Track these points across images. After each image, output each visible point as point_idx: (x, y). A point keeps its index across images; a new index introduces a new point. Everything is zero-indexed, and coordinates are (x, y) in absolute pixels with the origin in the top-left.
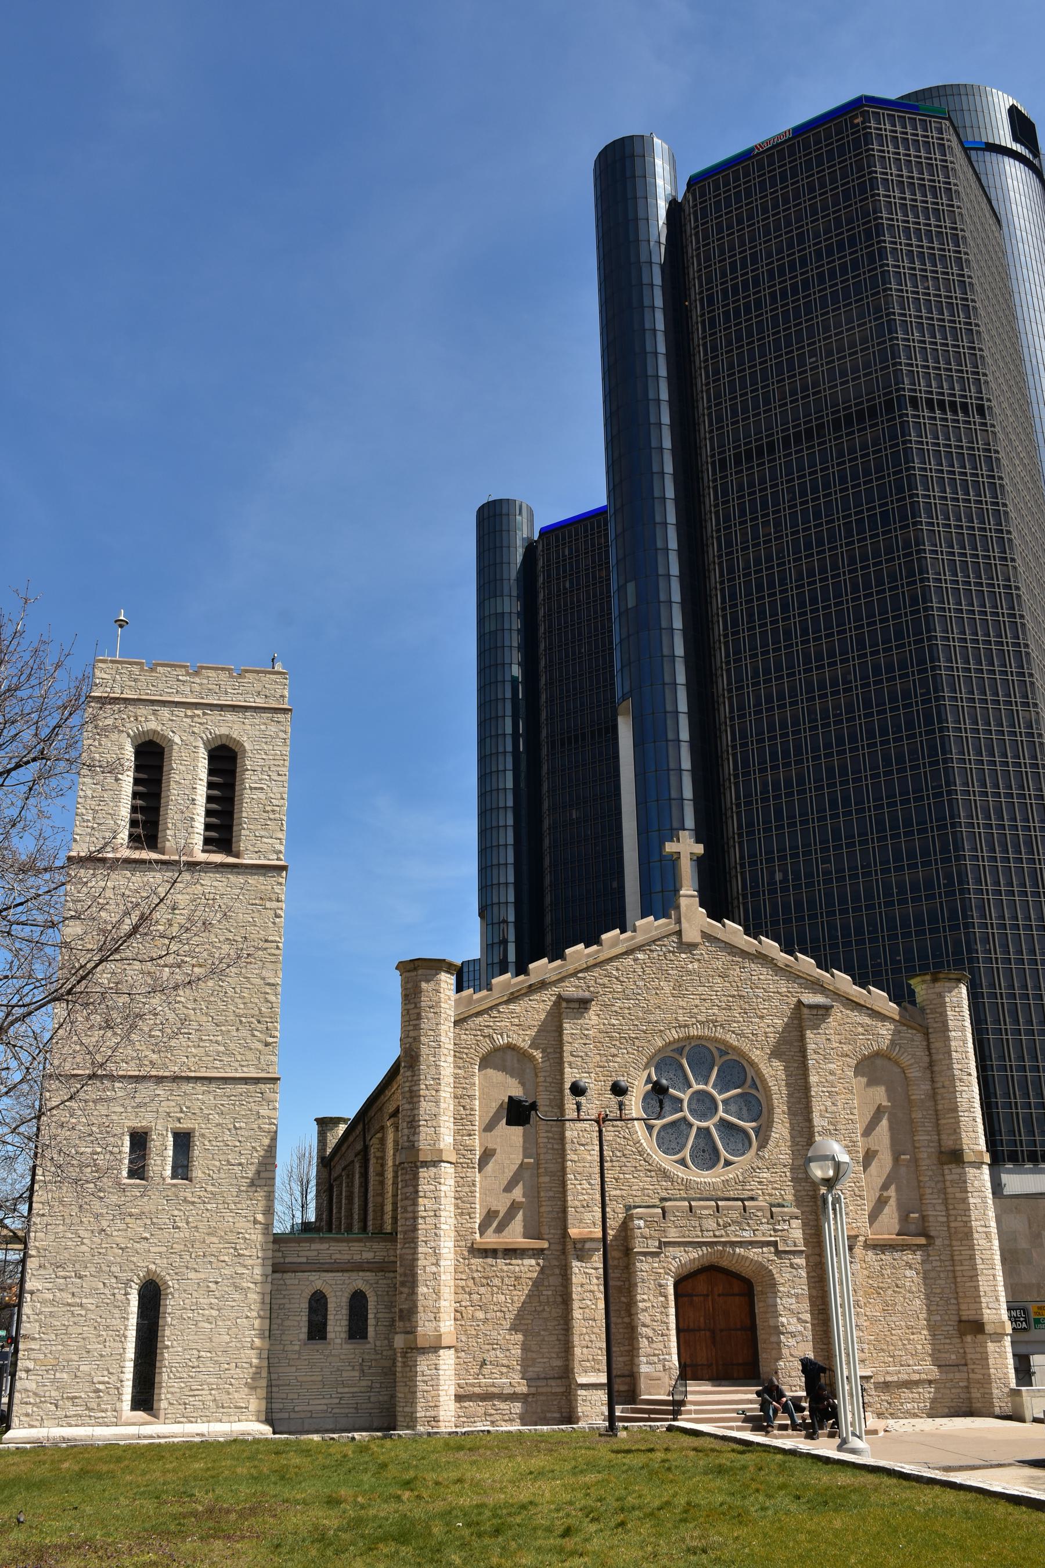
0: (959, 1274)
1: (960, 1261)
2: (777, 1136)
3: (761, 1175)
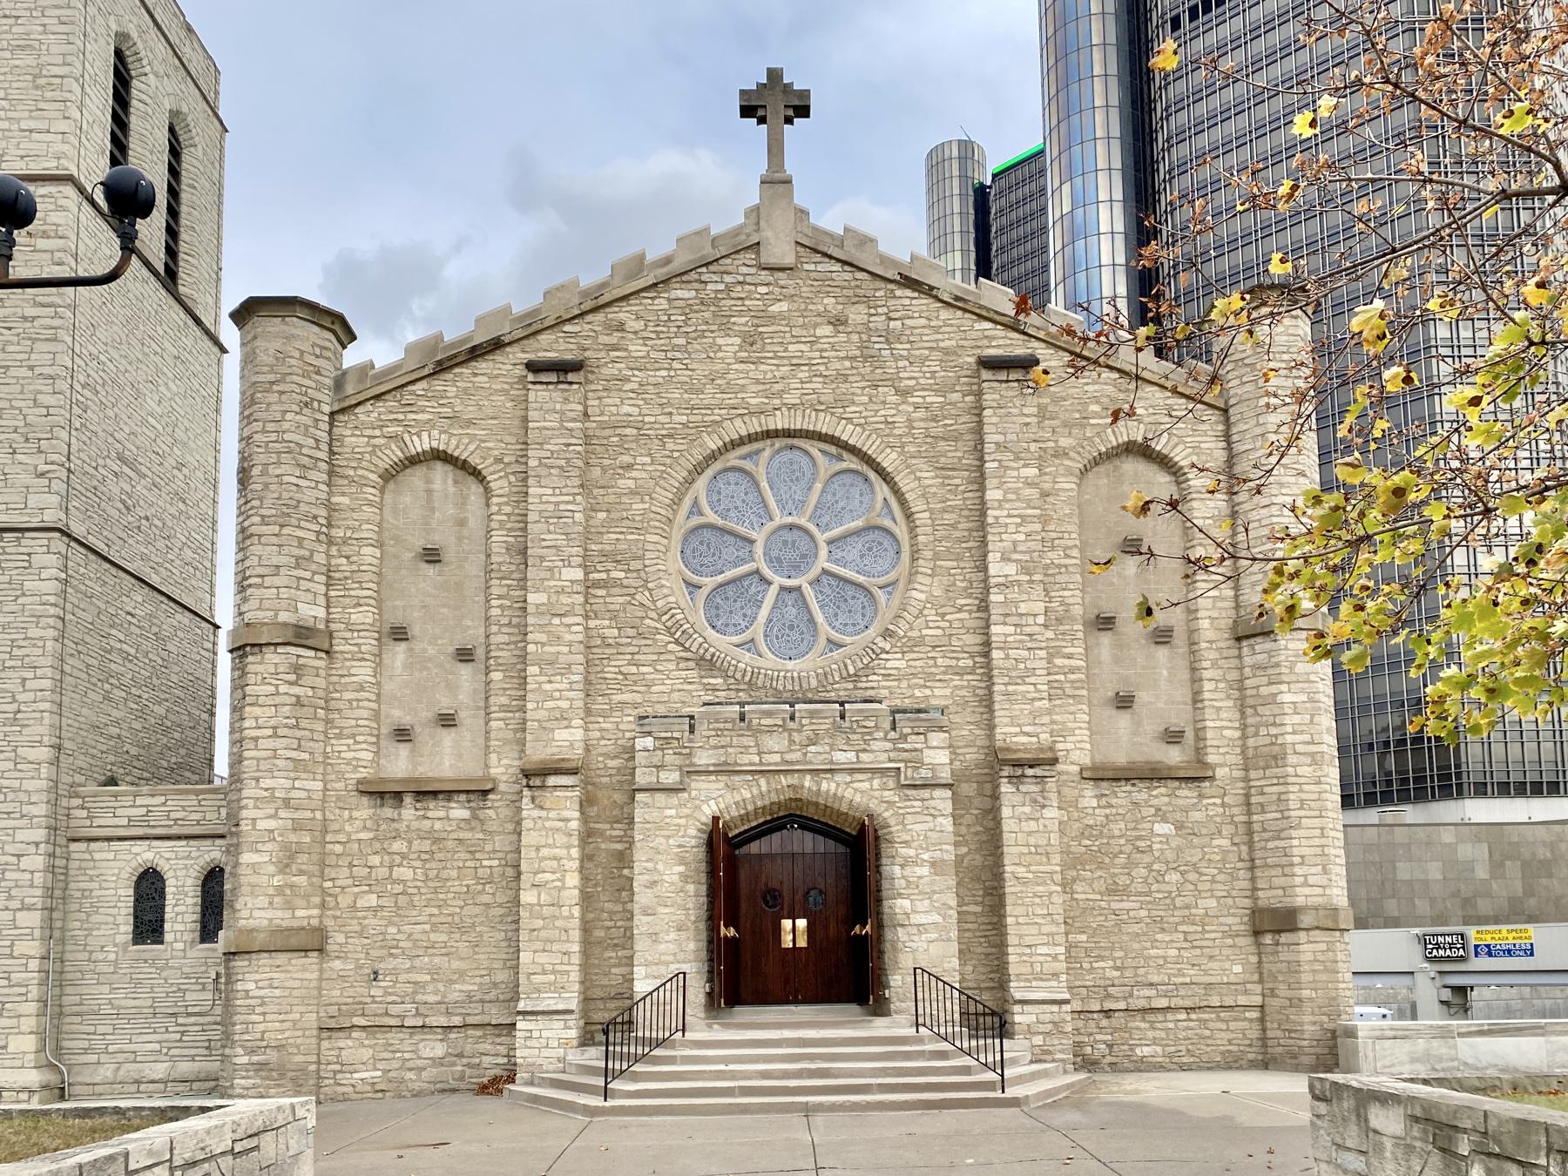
0: (1256, 827)
1: (1262, 805)
2: (923, 597)
3: (889, 665)
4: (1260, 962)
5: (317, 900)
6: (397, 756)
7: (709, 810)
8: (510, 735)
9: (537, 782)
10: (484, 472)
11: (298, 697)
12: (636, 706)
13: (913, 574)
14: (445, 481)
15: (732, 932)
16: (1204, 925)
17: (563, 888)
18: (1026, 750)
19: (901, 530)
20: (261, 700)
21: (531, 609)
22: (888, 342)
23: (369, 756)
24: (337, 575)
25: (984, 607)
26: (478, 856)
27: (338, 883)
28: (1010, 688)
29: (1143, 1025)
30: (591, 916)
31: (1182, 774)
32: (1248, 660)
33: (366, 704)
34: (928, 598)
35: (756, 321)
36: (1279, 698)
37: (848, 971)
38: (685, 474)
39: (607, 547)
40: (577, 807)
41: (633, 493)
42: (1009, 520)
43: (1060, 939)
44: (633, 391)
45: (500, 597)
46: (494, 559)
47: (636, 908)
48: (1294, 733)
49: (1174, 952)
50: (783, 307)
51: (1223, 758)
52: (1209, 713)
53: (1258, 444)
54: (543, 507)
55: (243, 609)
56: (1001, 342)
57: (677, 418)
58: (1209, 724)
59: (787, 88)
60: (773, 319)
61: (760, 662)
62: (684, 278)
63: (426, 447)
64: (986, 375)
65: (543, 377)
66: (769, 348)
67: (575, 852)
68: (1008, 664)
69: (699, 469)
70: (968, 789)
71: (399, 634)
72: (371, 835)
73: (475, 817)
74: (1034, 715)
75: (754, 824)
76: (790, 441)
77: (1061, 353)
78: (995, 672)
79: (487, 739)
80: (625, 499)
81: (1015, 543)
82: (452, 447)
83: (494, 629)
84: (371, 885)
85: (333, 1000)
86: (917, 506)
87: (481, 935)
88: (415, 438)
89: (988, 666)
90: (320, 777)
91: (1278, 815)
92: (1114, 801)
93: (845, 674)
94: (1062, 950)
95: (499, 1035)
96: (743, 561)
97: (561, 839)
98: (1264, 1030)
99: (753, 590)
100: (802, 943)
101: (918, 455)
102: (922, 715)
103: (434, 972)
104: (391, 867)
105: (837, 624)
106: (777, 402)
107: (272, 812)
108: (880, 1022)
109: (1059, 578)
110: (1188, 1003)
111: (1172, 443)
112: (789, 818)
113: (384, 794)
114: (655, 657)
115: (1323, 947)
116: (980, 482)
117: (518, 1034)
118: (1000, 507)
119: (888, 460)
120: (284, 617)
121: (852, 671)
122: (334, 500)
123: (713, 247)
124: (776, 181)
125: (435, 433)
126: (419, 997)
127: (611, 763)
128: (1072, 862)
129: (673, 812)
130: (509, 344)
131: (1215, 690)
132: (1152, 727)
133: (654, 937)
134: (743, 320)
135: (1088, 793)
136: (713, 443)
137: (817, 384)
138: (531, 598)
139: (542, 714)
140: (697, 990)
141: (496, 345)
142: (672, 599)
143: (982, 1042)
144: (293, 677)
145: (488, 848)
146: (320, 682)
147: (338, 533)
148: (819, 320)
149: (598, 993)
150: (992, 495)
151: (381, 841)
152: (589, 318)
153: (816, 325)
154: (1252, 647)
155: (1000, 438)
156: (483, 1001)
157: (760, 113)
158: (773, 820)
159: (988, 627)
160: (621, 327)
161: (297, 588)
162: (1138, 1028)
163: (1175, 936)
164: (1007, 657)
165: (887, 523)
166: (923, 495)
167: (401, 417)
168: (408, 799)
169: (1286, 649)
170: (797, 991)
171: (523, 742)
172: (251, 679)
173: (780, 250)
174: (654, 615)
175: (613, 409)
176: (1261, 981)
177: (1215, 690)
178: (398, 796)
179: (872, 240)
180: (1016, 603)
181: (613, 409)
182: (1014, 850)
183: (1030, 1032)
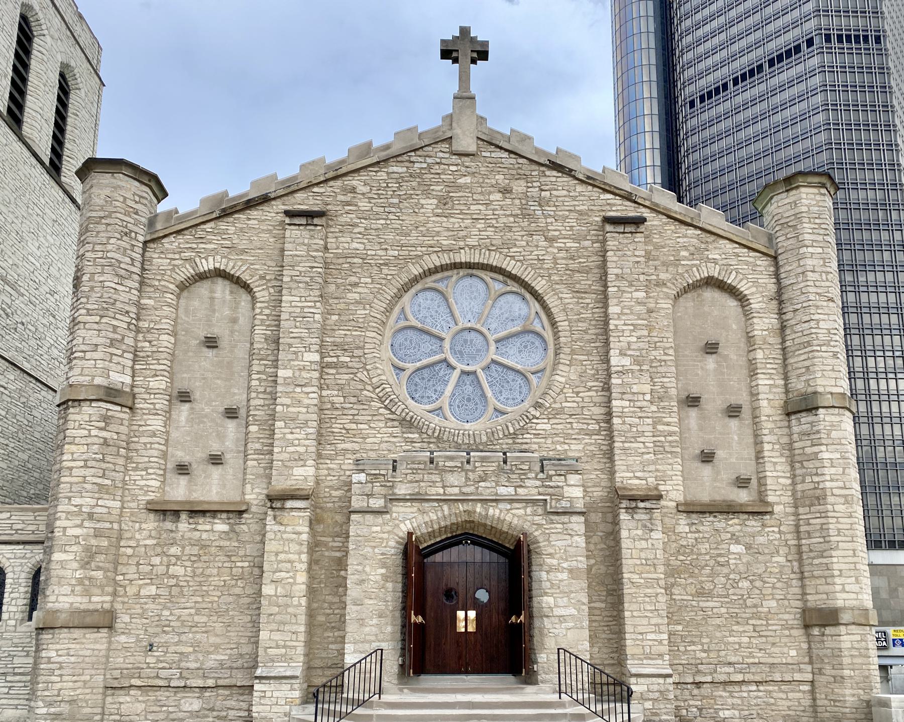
0: (804, 548)
1: (808, 532)
2: (563, 380)
3: (538, 427)
4: (810, 648)
5: (110, 589)
6: (179, 484)
7: (405, 528)
8: (261, 471)
10: (251, 286)
11: (105, 439)
12: (354, 452)
13: (556, 364)
14: (223, 291)
15: (420, 619)
16: (767, 620)
17: (295, 583)
18: (638, 490)
19: (548, 335)
20: (77, 440)
21: (280, 381)
22: (540, 205)
23: (158, 484)
24: (141, 354)
25: (607, 388)
26: (233, 559)
27: (127, 577)
28: (626, 445)
29: (724, 694)
30: (315, 605)
31: (750, 509)
32: (796, 429)
33: (156, 446)
35: (448, 189)
36: (820, 456)
37: (507, 650)
38: (395, 291)
39: (338, 340)
40: (307, 524)
41: (358, 302)
42: (625, 328)
43: (664, 628)
44: (360, 233)
45: (258, 373)
46: (256, 346)
47: (348, 600)
48: (832, 480)
49: (746, 640)
50: (468, 180)
51: (779, 497)
52: (768, 467)
53: (800, 279)
55: (70, 375)
56: (619, 208)
57: (391, 253)
58: (768, 474)
59: (473, 40)
61: (446, 424)
62: (399, 159)
63: (211, 267)
64: (609, 228)
65: (297, 221)
67: (304, 557)
69: (405, 288)
70: (596, 517)
71: (185, 397)
72: (154, 542)
73: (233, 530)
75: (438, 539)
76: (470, 271)
77: (660, 216)
78: (616, 433)
79: (245, 474)
80: (352, 307)
81: (629, 343)
83: (253, 395)
84: (152, 578)
85: (117, 666)
86: (559, 317)
87: (233, 617)
88: (203, 261)
89: (610, 429)
90: (119, 498)
91: (822, 540)
92: (701, 528)
93: (507, 433)
94: (665, 636)
95: (242, 694)
96: (436, 353)
97: (294, 547)
98: (814, 699)
99: (442, 373)
100: (471, 628)
101: (560, 282)
102: (563, 462)
103: (196, 645)
104: (168, 566)
105: (502, 398)
106: (462, 244)
107: (79, 522)
108: (530, 689)
110: (758, 678)
111: (738, 279)
112: (464, 535)
113: (166, 512)
114: (370, 418)
115: (858, 638)
117: (255, 694)
118: (619, 318)
119: (540, 285)
120: (98, 381)
121: (512, 431)
122: (142, 301)
123: (419, 139)
124: (464, 98)
125: (218, 258)
126: (183, 664)
127: (334, 493)
128: (672, 572)
129: (378, 529)
130: (274, 199)
131: (772, 450)
132: (727, 476)
133: (361, 622)
134: (439, 188)
135: (682, 522)
136: (416, 270)
137: (490, 232)
138: (281, 373)
139: (285, 456)
140: (392, 663)
141: (265, 199)
142: (383, 377)
143: (606, 706)
144: (102, 424)
145: (241, 553)
146: (124, 429)
147: (144, 325)
148: (492, 189)
149: (317, 663)
150: (613, 310)
151: (162, 544)
152: (331, 183)
153: (490, 193)
154: (799, 419)
155: (619, 271)
156: (231, 668)
157: (454, 55)
158: (452, 537)
159: (610, 401)
160: (353, 190)
161: (110, 361)
162: (721, 697)
163: (747, 628)
164: (624, 423)
165: (538, 327)
166: (564, 310)
167: (194, 246)
168: (184, 516)
169: (824, 420)
170: (467, 665)
171: (269, 477)
172: (71, 425)
173: (467, 143)
175: (346, 245)
176: (811, 663)
177: (772, 450)
178: (176, 513)
179: (530, 138)
180: (630, 385)
181: (346, 245)
182: (630, 562)
183: (643, 698)
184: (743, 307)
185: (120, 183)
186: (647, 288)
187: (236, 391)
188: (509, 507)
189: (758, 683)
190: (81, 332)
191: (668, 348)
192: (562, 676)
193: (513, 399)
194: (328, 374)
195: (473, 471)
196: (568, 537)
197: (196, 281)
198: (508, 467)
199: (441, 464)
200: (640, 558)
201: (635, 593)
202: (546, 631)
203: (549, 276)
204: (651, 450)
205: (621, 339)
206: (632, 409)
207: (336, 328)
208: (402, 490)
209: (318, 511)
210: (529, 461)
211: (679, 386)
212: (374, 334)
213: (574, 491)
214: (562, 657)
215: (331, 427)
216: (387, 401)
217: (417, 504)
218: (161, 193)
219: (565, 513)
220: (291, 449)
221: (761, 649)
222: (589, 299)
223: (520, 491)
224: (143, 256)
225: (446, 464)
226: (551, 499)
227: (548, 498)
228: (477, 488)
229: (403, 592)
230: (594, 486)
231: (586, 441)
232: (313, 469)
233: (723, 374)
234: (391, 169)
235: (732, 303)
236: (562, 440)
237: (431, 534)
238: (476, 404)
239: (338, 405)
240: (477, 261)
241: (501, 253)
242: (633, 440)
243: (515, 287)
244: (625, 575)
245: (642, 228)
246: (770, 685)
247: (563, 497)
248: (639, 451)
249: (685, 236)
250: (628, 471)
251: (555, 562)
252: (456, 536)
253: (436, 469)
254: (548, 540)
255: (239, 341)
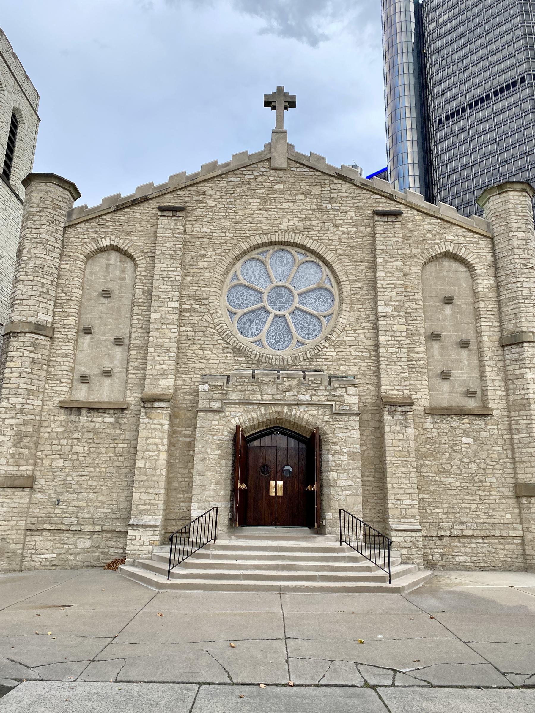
0: (515, 441)
1: (518, 429)
2: (345, 321)
3: (328, 354)
4: (520, 513)
5: (32, 461)
7: (235, 422)
8: (137, 381)
9: (149, 405)
10: (134, 256)
11: (33, 358)
13: (340, 310)
14: (116, 260)
15: (244, 486)
16: (490, 492)
17: (158, 460)
18: (397, 398)
19: (335, 290)
20: (15, 359)
21: (152, 321)
22: (330, 203)
23: (66, 389)
24: (60, 301)
25: (375, 327)
26: (116, 442)
27: (44, 453)
28: (389, 367)
29: (459, 545)
30: (172, 475)
31: (476, 413)
32: (508, 357)
33: (67, 363)
34: (349, 322)
35: (267, 192)
36: (525, 376)
37: (304, 510)
38: (231, 260)
39: (192, 293)
40: (168, 418)
41: (205, 268)
42: (388, 286)
43: (415, 496)
44: (208, 222)
45: (138, 315)
46: (136, 297)
47: (195, 472)
49: (474, 506)
50: (281, 186)
51: (496, 403)
52: (489, 383)
53: (509, 253)
54: (161, 273)
55: (12, 315)
56: (384, 205)
57: (228, 235)
58: (489, 388)
59: (286, 95)
60: (276, 191)
62: (235, 172)
63: (108, 244)
64: (377, 218)
65: (166, 214)
66: (273, 204)
67: (165, 441)
68: (389, 355)
69: (238, 258)
70: (367, 417)
71: (87, 331)
72: (63, 429)
73: (117, 422)
74: (401, 380)
75: (258, 430)
76: (282, 247)
77: (412, 210)
78: (381, 359)
79: (126, 383)
80: (201, 271)
81: (391, 296)
82: (120, 244)
83: (134, 330)
84: (61, 454)
85: (35, 515)
86: (343, 278)
87: (115, 483)
88: (103, 240)
89: (378, 356)
90: (41, 399)
91: (527, 435)
92: (442, 426)
93: (305, 358)
94: (416, 502)
95: (119, 537)
96: (257, 302)
97: (159, 434)
98: (524, 550)
102: (344, 379)
103: (89, 501)
104: (72, 446)
105: (302, 334)
106: (276, 228)
107: (14, 415)
108: (320, 538)
109: (412, 314)
110: (483, 533)
111: (467, 253)
112: (275, 428)
113: (71, 408)
114: (212, 346)
116: (374, 267)
117: (129, 537)
118: (384, 280)
119: (329, 257)
120: (30, 319)
121: (309, 356)
122: (62, 266)
123: (249, 159)
124: (280, 132)
125: (113, 238)
126: (80, 515)
127: (187, 397)
128: (421, 456)
129: (216, 423)
130: (151, 199)
131: (492, 371)
132: (460, 389)
133: (203, 487)
134: (262, 191)
135: (428, 421)
136: (245, 246)
137: (296, 220)
138: (153, 315)
139: (154, 372)
140: (224, 517)
142: (222, 319)
144: (32, 349)
145: (122, 438)
146: (46, 352)
148: (297, 192)
149: (173, 516)
151: (68, 432)
152: (189, 189)
153: (296, 195)
154: (510, 350)
155: (384, 247)
156: (112, 518)
157: (273, 104)
158: (267, 429)
159: (377, 337)
160: (204, 193)
161: (39, 306)
162: (457, 546)
163: (475, 497)
165: (328, 286)
166: (346, 274)
167: (97, 230)
168: (84, 412)
169: (528, 351)
170: (277, 519)
171: (143, 385)
172: (11, 349)
173: (281, 161)
174: (212, 326)
176: (521, 523)
177: (492, 371)
178: (79, 410)
179: (324, 159)
180: (392, 326)
182: (391, 449)
183: (400, 547)
184: (470, 272)
185: (50, 189)
186: (404, 258)
187: (122, 327)
188: (306, 409)
189: (483, 537)
190: (21, 287)
191: (418, 300)
192: (343, 529)
193: (310, 334)
194: (184, 316)
195: (282, 384)
196: (347, 431)
197: (98, 253)
198: (306, 382)
199: (260, 379)
200: (398, 446)
201: (395, 471)
202: (332, 497)
203: (336, 251)
204: (406, 371)
205: (386, 293)
206: (393, 342)
207: (190, 285)
208: (233, 396)
209: (176, 409)
210: (321, 377)
211: (426, 326)
212: (215, 290)
213: (352, 399)
214: (342, 515)
215: (186, 352)
216: (224, 335)
217: (243, 406)
218: (76, 194)
219: (345, 414)
220: (158, 367)
221: (485, 513)
222: (363, 266)
223: (314, 398)
224: (63, 236)
225: (264, 379)
226: (336, 404)
227: (333, 403)
228: (285, 396)
229: (232, 467)
230: (366, 395)
231: (361, 364)
232: (173, 380)
233: (457, 318)
234: (229, 179)
235: (463, 269)
236: (344, 363)
237: (253, 427)
238: (285, 337)
239: (190, 338)
240: (286, 240)
241: (303, 235)
242: (393, 363)
243: (312, 258)
244: (388, 458)
245: (400, 219)
246: (492, 539)
247: (344, 403)
248: (398, 371)
249: (429, 224)
250: (390, 385)
251: (338, 448)
252: (270, 428)
253: (257, 382)
254: (334, 433)
255: (125, 293)
